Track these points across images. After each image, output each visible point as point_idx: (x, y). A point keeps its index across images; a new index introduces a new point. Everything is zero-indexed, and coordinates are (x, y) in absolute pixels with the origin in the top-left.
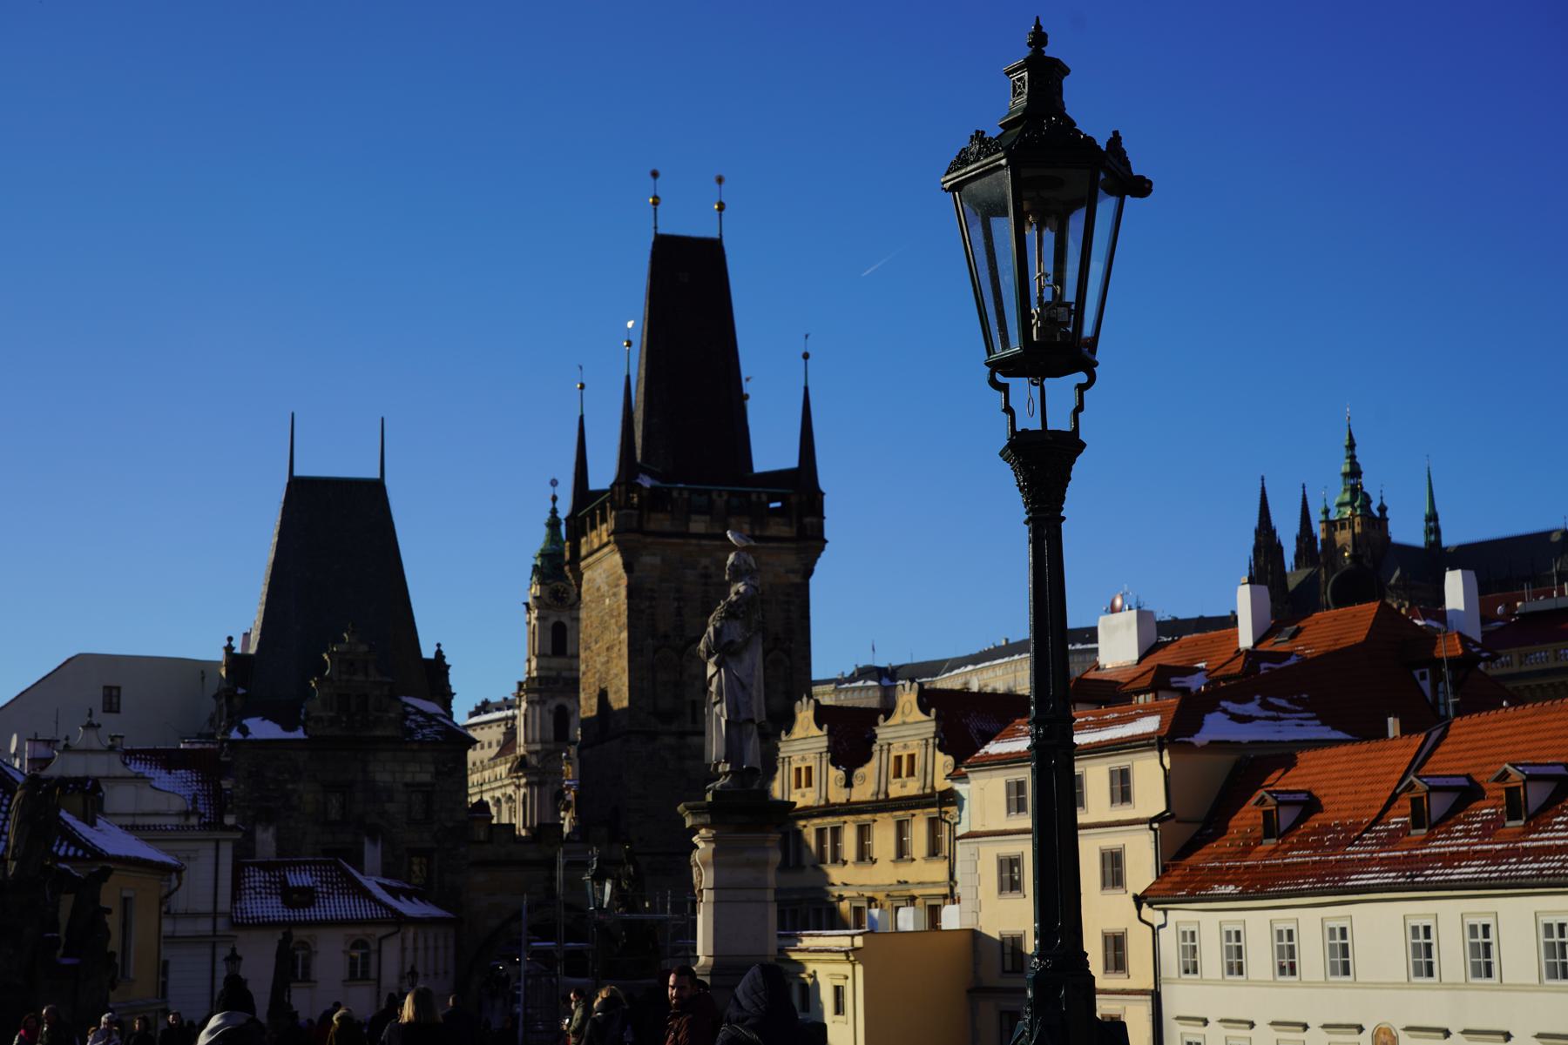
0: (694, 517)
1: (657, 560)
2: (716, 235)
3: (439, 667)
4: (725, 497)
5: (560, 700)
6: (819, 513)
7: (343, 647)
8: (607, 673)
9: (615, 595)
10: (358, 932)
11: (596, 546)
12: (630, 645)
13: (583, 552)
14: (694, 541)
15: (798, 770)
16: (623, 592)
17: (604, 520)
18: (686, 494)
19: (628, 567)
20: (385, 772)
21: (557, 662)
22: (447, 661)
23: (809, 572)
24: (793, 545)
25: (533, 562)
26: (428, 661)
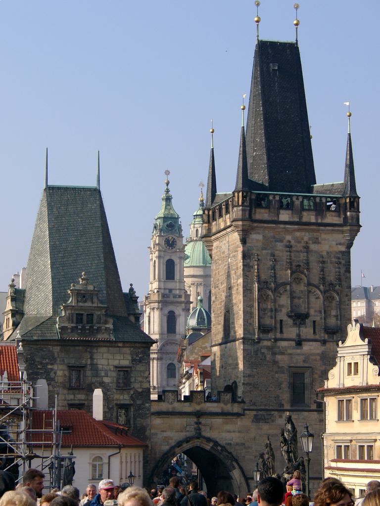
0: (282, 211)
2: (295, 42)
4: (301, 199)
5: (171, 308)
6: (358, 211)
7: (77, 287)
9: (234, 256)
10: (97, 452)
11: (222, 227)
12: (244, 287)
13: (214, 230)
14: (282, 226)
15: (350, 364)
16: (240, 255)
17: (227, 212)
19: (244, 241)
21: (170, 285)
22: (137, 294)
23: (350, 245)
25: (154, 222)
26: (125, 294)
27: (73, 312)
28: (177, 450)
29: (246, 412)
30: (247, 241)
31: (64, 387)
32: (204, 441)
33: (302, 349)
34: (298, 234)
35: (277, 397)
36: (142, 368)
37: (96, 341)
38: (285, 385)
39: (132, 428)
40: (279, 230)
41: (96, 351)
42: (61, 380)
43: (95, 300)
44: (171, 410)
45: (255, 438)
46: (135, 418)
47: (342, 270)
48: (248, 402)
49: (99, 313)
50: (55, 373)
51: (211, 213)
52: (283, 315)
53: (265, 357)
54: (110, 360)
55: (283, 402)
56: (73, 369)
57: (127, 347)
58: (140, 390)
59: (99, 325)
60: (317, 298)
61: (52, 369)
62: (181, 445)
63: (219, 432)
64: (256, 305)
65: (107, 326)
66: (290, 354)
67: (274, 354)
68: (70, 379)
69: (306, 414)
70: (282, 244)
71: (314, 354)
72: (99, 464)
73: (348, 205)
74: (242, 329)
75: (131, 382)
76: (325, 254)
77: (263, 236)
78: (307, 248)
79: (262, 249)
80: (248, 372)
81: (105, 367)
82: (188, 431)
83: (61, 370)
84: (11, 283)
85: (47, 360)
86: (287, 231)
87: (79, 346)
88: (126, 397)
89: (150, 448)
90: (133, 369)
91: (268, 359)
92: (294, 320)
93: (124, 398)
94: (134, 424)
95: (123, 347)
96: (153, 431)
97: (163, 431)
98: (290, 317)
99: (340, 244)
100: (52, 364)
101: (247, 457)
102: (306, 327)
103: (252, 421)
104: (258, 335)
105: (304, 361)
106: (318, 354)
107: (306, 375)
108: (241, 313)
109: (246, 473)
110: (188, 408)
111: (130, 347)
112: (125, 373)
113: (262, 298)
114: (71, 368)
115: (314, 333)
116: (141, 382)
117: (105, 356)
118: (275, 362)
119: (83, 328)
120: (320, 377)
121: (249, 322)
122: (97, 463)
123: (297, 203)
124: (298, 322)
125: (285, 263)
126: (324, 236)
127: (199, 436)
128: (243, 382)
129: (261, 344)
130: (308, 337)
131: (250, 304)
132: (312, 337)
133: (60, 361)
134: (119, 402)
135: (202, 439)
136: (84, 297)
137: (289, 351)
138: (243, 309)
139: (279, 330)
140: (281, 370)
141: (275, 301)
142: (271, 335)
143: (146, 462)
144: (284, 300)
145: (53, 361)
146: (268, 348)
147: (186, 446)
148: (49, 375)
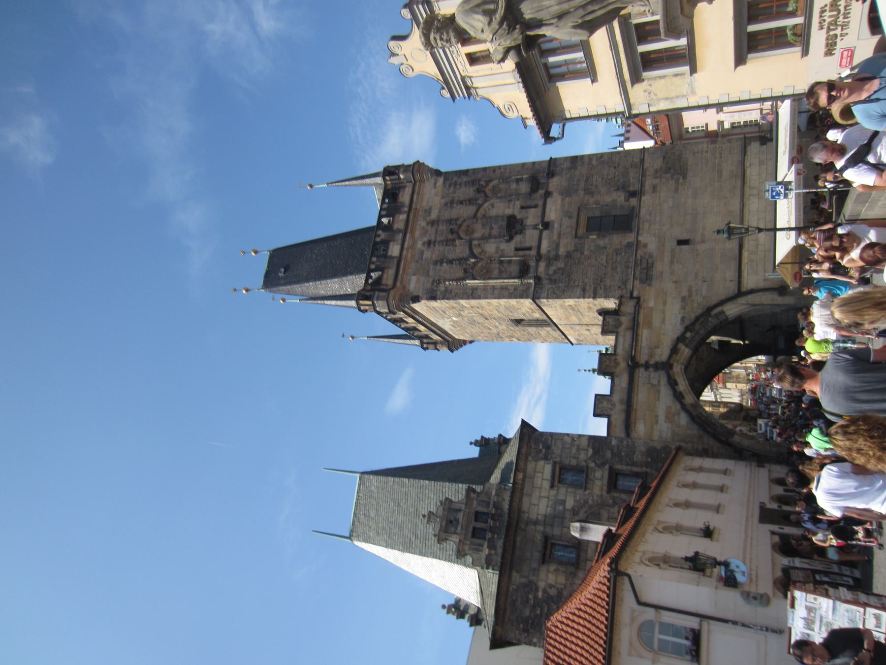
0: (389, 253)
1: (414, 279)
3: (483, 443)
4: (380, 232)
6: (397, 168)
8: (504, 320)
10: (626, 635)
12: (468, 298)
14: (404, 252)
16: (434, 304)
17: (402, 320)
18: (374, 259)
19: (416, 299)
20: (540, 501)
22: (479, 438)
23: (438, 173)
24: (418, 184)
27: (468, 542)
28: (689, 399)
29: (635, 294)
30: (415, 294)
31: (574, 575)
32: (678, 357)
33: (553, 221)
34: (417, 233)
35: (617, 252)
36: (559, 444)
37: (509, 516)
38: (601, 243)
39: (648, 470)
40: (409, 255)
41: (526, 515)
42: (561, 579)
43: (457, 506)
44: (624, 407)
45: (675, 282)
46: (634, 464)
47: (465, 179)
48: (620, 292)
49: (475, 502)
50: (551, 586)
51: (425, 341)
52: (508, 248)
53: (559, 269)
54: (543, 494)
55: (625, 242)
56: (547, 556)
57: (526, 465)
58: (590, 451)
59: (491, 506)
60: (493, 207)
61: (545, 591)
62: (681, 393)
63: (664, 334)
64: (492, 282)
65: (494, 493)
66: (559, 236)
67: (557, 257)
68: (561, 563)
69: (643, 211)
70: (425, 252)
71: (563, 206)
72: (660, 633)
73: (392, 177)
74: (522, 300)
75: (577, 465)
76: (443, 201)
77: (414, 275)
78: (433, 223)
79: (428, 275)
80: (578, 291)
81: (551, 503)
82: (659, 382)
83: (547, 575)
84: (446, 610)
85: (530, 596)
86: (413, 247)
87: (514, 542)
88: (598, 474)
89: (683, 444)
90: (558, 459)
91: (563, 266)
92: (516, 233)
93: (600, 478)
94: (642, 466)
95: (525, 472)
96: (656, 436)
97: (657, 422)
98: (511, 238)
99: (435, 184)
100: (537, 589)
101: (704, 294)
102: (527, 218)
103: (650, 285)
104: (530, 278)
105: (570, 217)
106: (563, 200)
107: (591, 214)
108: (503, 302)
109: (731, 294)
110: (623, 381)
111: (527, 458)
112: (563, 474)
113: (486, 274)
114: (546, 558)
115: (536, 206)
116: (578, 449)
117: (534, 500)
118: (569, 255)
119: (492, 530)
120: (593, 196)
121: (511, 291)
122: (657, 636)
123: (382, 235)
124: (518, 227)
125: (448, 248)
126: (424, 204)
127: (666, 366)
128: (591, 300)
129: (543, 276)
130: (540, 214)
131: (489, 290)
132: (540, 209)
133: (534, 575)
134: (605, 488)
135: (671, 361)
136: (451, 522)
137: (555, 238)
138: (495, 298)
139: (527, 252)
140: (579, 249)
141: (490, 259)
142: (532, 264)
143: (705, 453)
144: (491, 248)
145: (531, 586)
146: (548, 266)
147: (683, 385)
148: (552, 597)
